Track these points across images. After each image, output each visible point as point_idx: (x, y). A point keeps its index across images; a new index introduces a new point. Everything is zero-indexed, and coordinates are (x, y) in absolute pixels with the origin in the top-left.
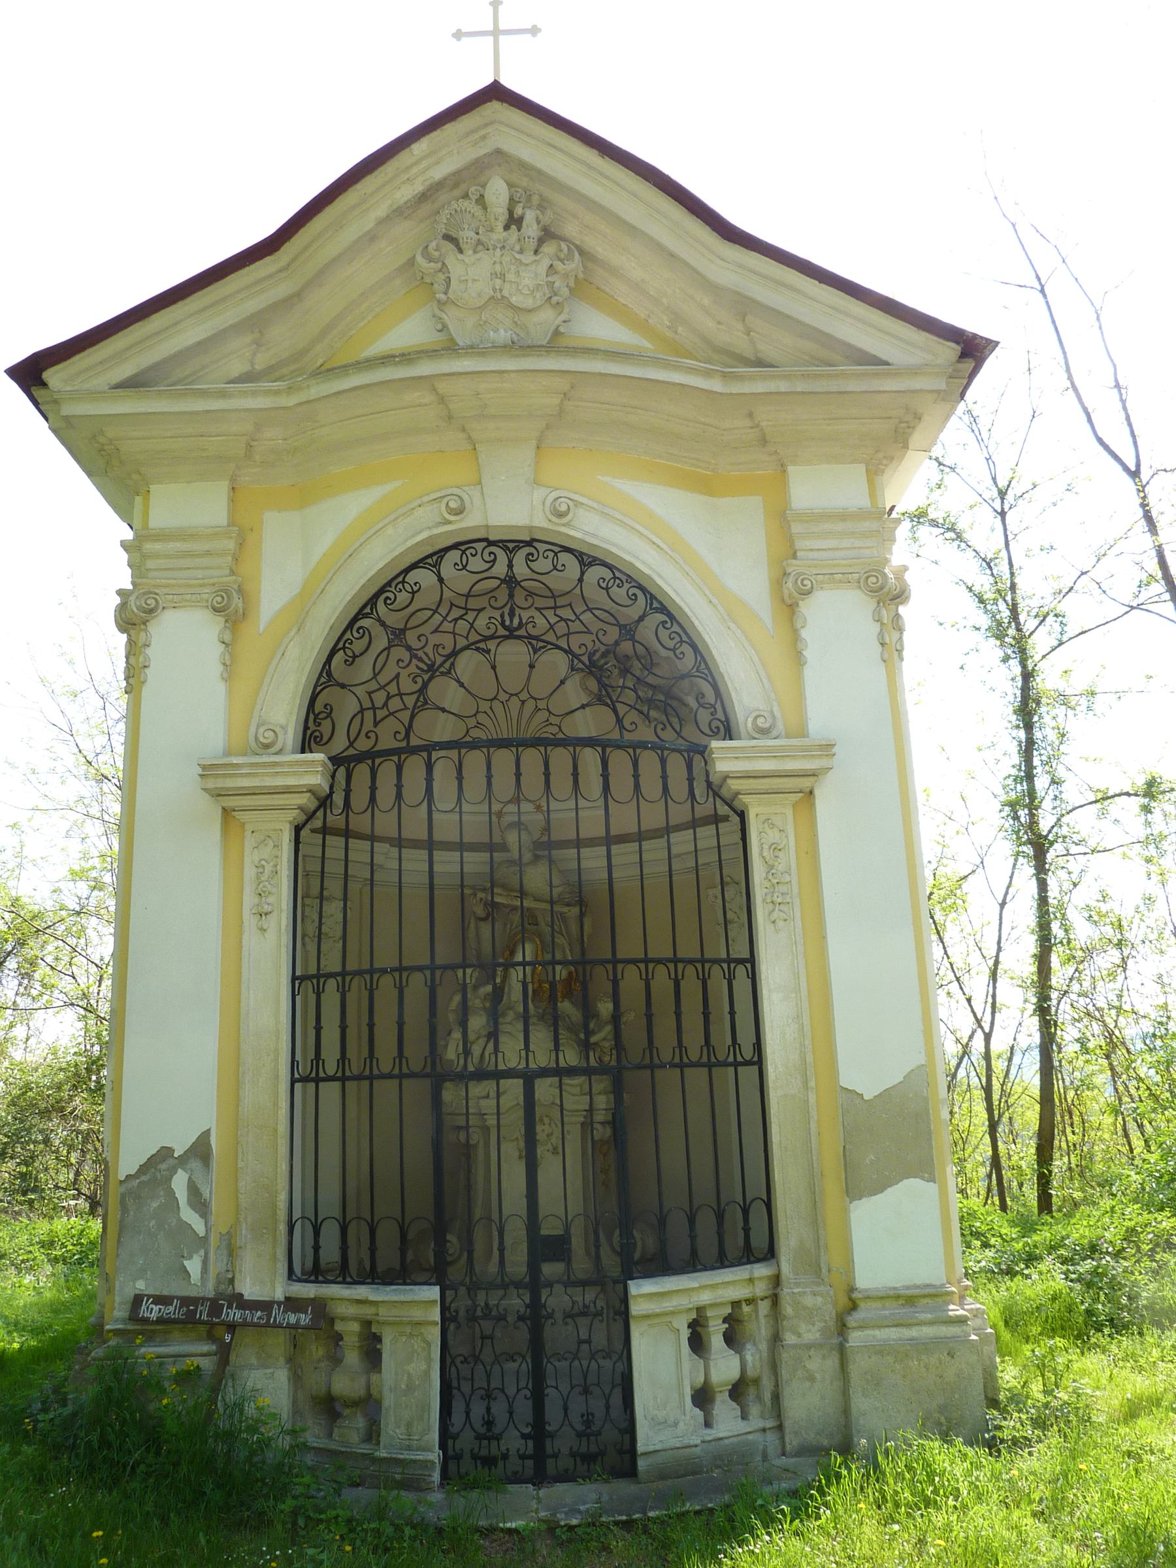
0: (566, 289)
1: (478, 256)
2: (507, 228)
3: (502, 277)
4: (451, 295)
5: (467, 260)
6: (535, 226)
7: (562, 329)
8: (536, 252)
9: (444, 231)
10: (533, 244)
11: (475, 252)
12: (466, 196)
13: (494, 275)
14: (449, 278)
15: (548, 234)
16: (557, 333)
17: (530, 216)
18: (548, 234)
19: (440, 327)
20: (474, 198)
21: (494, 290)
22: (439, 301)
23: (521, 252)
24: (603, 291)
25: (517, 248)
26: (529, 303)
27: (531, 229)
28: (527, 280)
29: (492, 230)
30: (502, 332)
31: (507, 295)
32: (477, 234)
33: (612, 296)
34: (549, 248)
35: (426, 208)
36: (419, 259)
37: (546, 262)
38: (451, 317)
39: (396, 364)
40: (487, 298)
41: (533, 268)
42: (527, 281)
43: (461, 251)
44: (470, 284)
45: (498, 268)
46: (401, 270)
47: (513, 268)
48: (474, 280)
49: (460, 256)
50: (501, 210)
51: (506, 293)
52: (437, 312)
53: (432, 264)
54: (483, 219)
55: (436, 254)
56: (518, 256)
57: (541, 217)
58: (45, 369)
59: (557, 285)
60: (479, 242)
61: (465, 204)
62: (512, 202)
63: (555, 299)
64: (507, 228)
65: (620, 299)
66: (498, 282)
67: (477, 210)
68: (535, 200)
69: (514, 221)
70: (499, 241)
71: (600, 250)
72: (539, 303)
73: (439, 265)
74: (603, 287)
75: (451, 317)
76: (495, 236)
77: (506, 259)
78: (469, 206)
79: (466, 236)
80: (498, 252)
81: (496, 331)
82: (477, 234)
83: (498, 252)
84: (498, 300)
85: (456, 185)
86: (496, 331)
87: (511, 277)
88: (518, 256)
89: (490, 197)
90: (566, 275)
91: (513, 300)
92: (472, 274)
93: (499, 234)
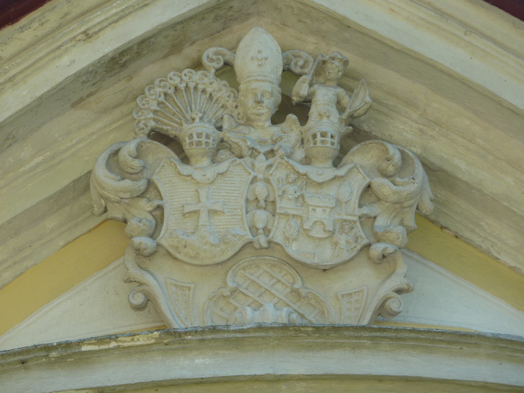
0: (400, 230)
1: (222, 167)
2: (277, 118)
3: (270, 205)
4: (164, 239)
5: (198, 175)
6: (335, 116)
7: (393, 305)
8: (337, 162)
9: (152, 124)
10: (331, 146)
11: (214, 161)
12: (198, 65)
13: (252, 202)
14: (160, 208)
15: (355, 134)
16: (382, 311)
17: (324, 98)
18: (355, 134)
19: (139, 299)
20: (212, 66)
21: (253, 229)
22: (138, 251)
23: (307, 161)
24: (469, 242)
25: (300, 154)
26: (326, 255)
27: (325, 120)
28: (320, 210)
29: (248, 122)
30: (270, 308)
31: (278, 238)
32: (220, 129)
33: (487, 253)
34: (362, 157)
35: (112, 91)
36: (102, 174)
37: (358, 182)
38: (160, 280)
39: (52, 364)
40: (240, 244)
41: (332, 190)
42: (319, 215)
43: (185, 159)
44: (204, 218)
45: (261, 190)
46: (58, 200)
47: (291, 189)
48: (212, 212)
49: (185, 169)
50: (267, 87)
51: (278, 237)
52: (135, 272)
53: (127, 183)
54: (230, 103)
55: (137, 164)
56: (302, 169)
57: (346, 100)
58: (295, 114)
59: (380, 222)
60: (222, 144)
61: (196, 77)
62: (289, 75)
63: (377, 249)
64: (277, 118)
65: (503, 258)
66: (261, 217)
67: (219, 88)
68: (334, 69)
69: (292, 108)
70: (262, 142)
71: (463, 165)
72: (346, 256)
73: (142, 184)
74: (467, 234)
75: (160, 280)
76: (254, 134)
77: (279, 174)
78: (206, 80)
79: (196, 130)
80: (261, 162)
81: (258, 306)
82: (220, 129)
83: (261, 162)
84: (258, 249)
85: (176, 48)
86: (258, 306)
87: (285, 205)
88: (302, 169)
89: (245, 63)
90: (398, 206)
91: (294, 249)
92: (207, 201)
93: (264, 131)
